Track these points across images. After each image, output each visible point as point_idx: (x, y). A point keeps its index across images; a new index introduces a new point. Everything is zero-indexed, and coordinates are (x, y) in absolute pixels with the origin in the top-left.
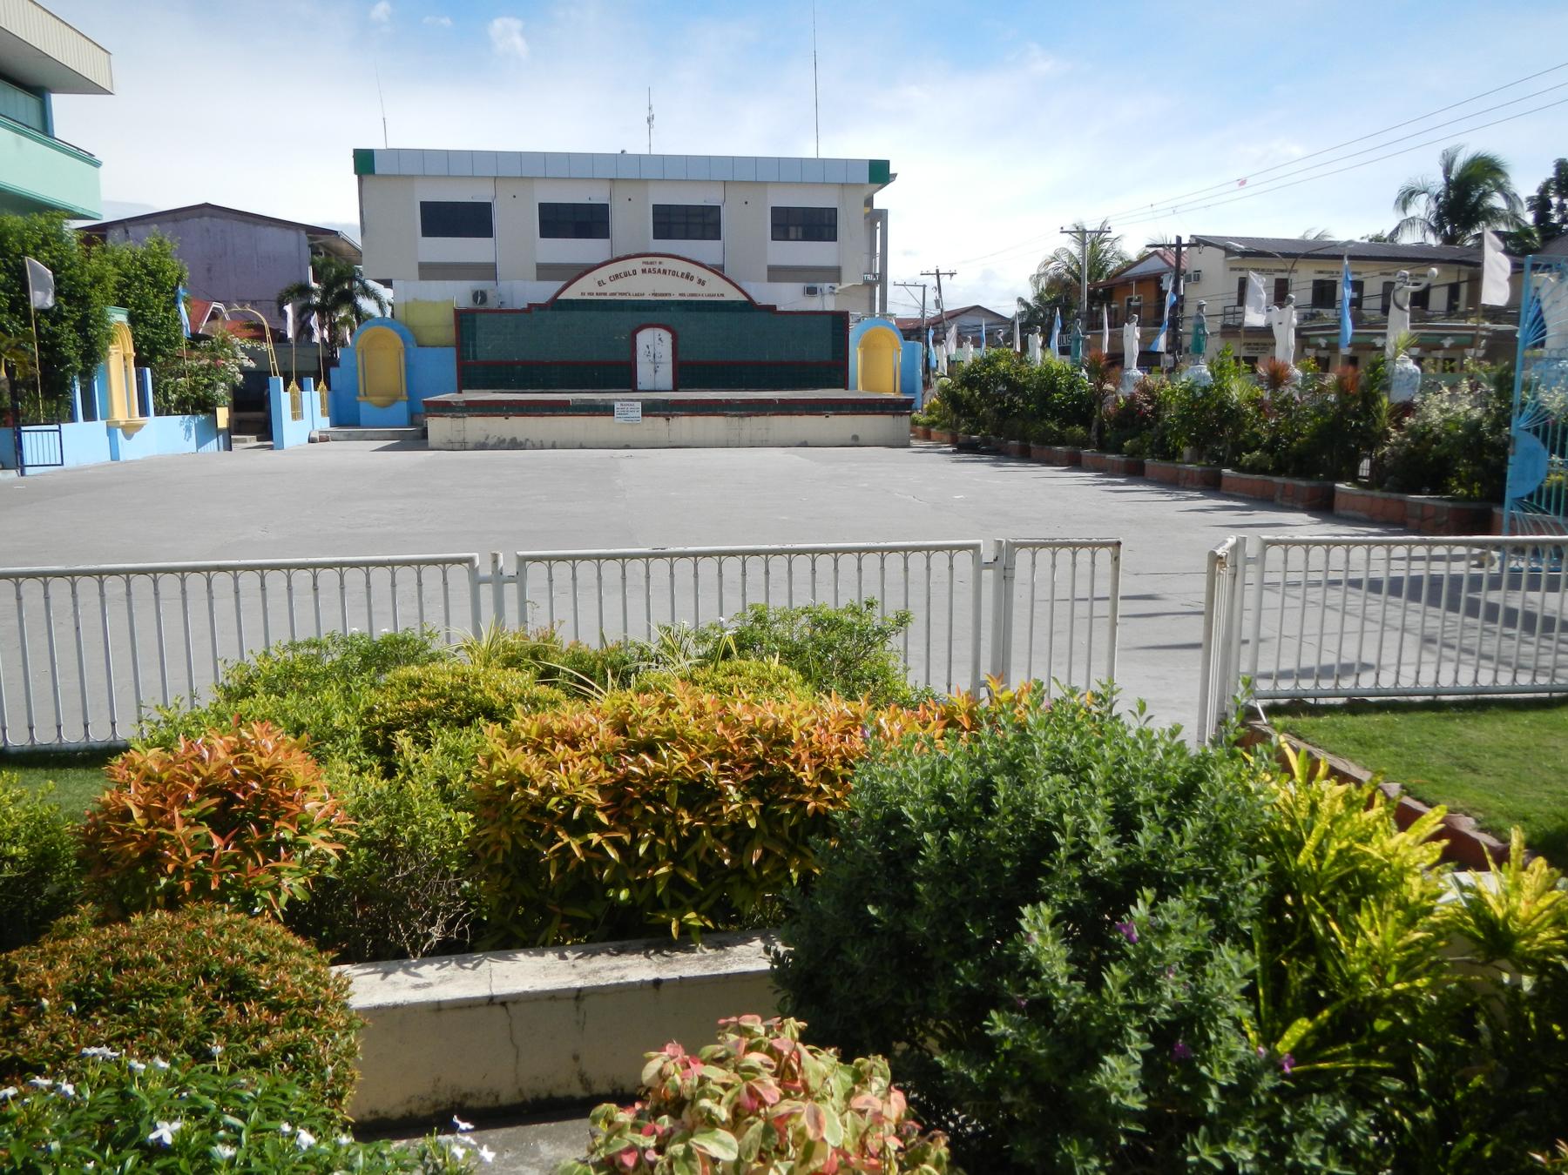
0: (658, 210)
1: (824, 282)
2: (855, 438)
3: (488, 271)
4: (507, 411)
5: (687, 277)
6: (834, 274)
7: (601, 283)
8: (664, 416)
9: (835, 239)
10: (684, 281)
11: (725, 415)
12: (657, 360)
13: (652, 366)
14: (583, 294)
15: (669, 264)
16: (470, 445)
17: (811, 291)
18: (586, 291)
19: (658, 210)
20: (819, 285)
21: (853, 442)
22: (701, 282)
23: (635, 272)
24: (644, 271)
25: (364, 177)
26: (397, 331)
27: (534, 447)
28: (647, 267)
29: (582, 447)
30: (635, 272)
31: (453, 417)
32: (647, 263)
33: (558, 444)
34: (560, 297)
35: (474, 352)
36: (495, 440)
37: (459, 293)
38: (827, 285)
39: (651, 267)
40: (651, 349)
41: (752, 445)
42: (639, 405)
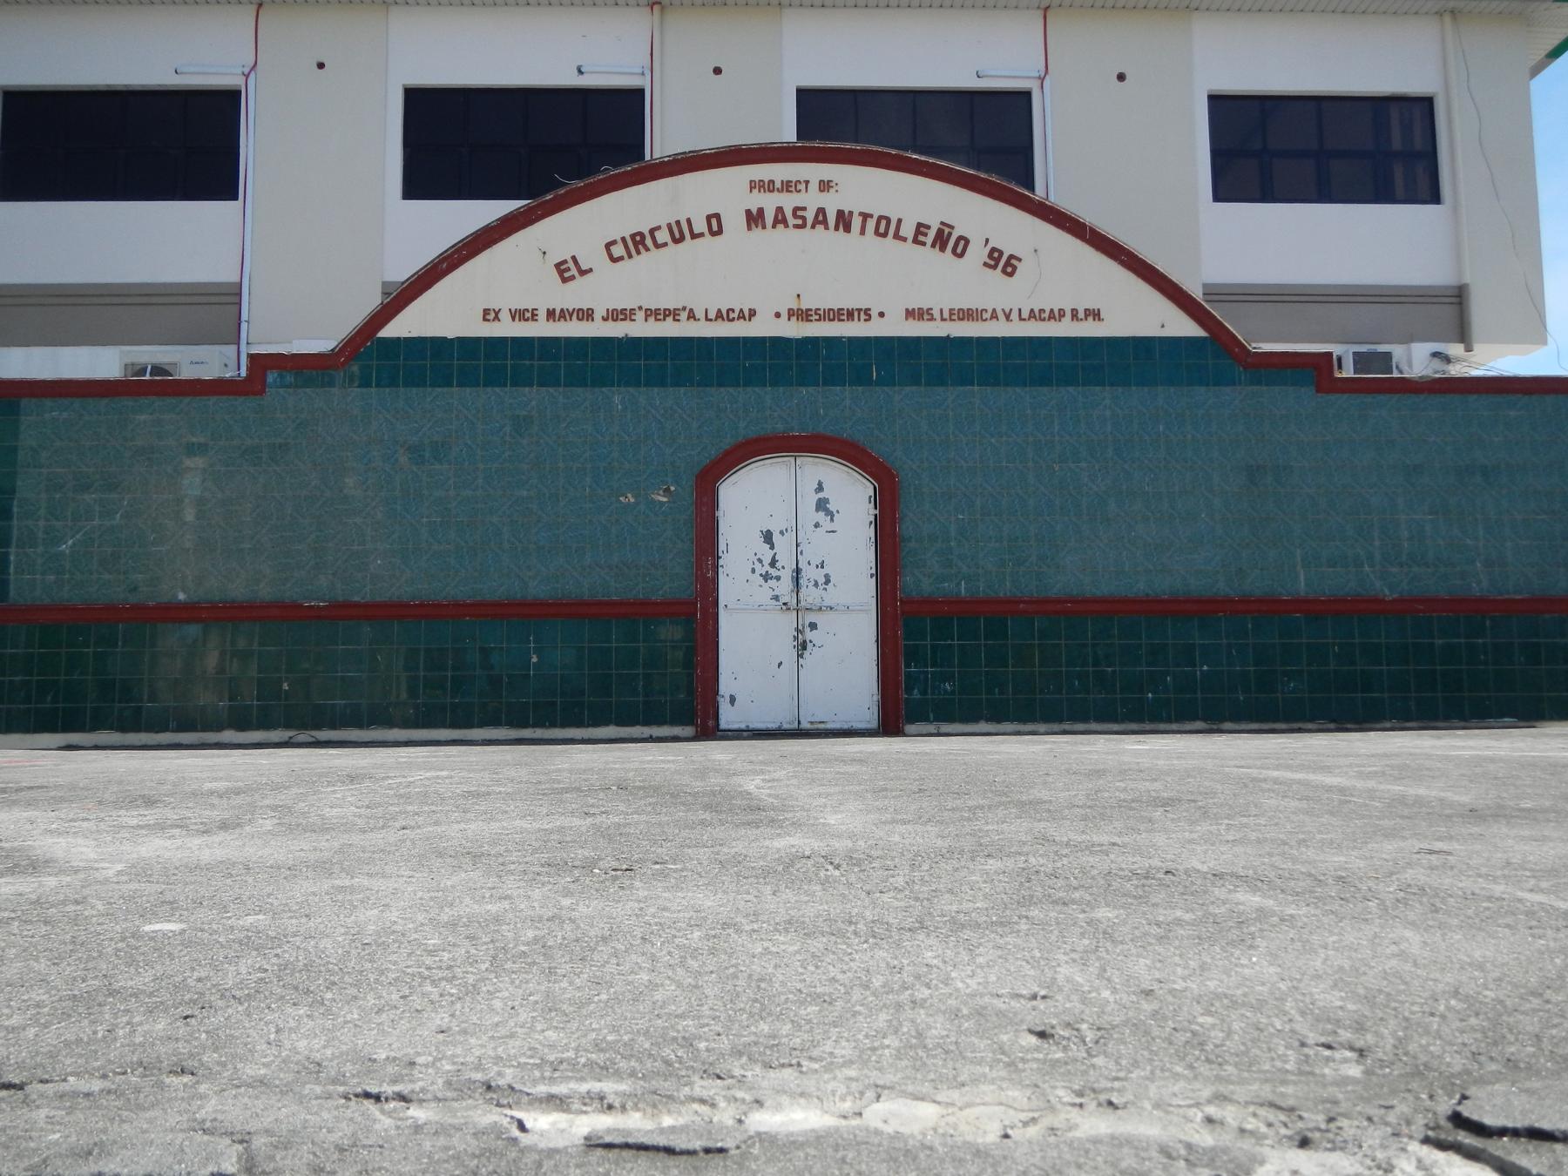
1: (1409, 339)
5: (941, 240)
9: (1433, 196)
10: (928, 254)
12: (810, 595)
13: (788, 622)
14: (489, 315)
18: (506, 303)
22: (1002, 262)
23: (715, 226)
24: (754, 219)
28: (769, 203)
32: (768, 187)
34: (390, 331)
39: (788, 201)
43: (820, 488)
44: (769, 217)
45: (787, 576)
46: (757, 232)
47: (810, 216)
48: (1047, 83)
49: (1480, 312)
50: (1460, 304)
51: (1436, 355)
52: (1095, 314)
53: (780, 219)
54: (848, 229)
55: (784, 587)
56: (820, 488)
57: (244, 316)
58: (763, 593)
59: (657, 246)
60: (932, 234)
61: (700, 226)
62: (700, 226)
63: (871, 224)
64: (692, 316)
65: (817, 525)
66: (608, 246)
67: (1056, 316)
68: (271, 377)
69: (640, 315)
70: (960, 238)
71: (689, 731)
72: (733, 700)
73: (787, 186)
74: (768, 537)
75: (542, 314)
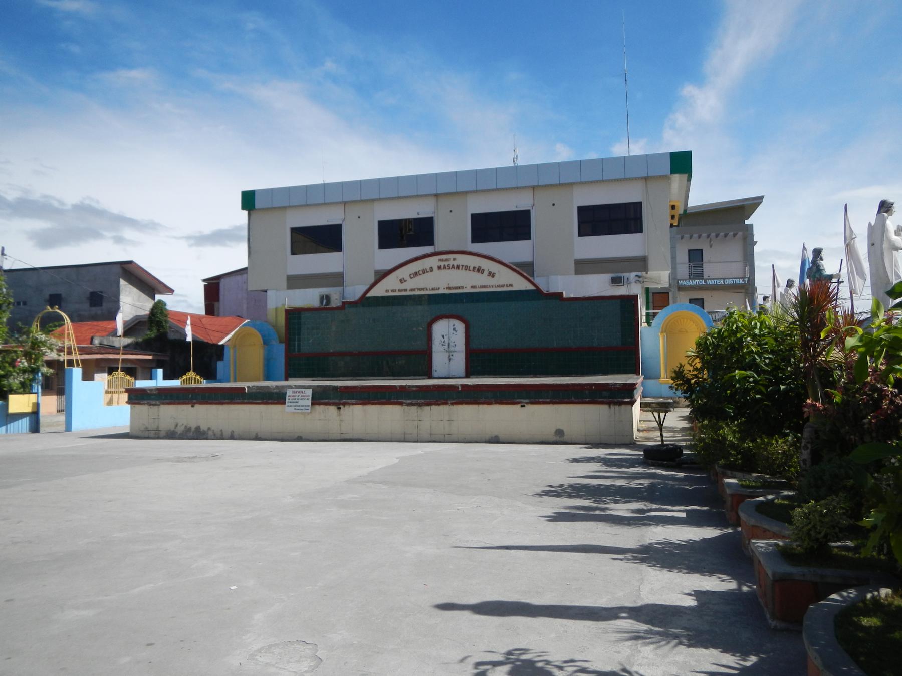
0: (476, 218)
1: (631, 272)
2: (559, 432)
3: (337, 279)
4: (192, 399)
5: (478, 271)
6: (641, 263)
7: (402, 281)
8: (333, 404)
9: (640, 230)
10: (476, 275)
11: (401, 404)
12: (452, 349)
14: (387, 291)
15: (462, 260)
16: (163, 434)
17: (616, 281)
18: (390, 288)
19: (476, 218)
20: (626, 275)
21: (557, 438)
22: (492, 275)
23: (432, 270)
25: (251, 212)
26: (258, 330)
27: (215, 438)
28: (442, 264)
29: (257, 438)
30: (432, 270)
31: (150, 404)
33: (236, 434)
34: (369, 295)
35: (299, 345)
36: (183, 428)
37: (308, 298)
38: (633, 275)
39: (446, 263)
40: (446, 339)
41: (433, 439)
42: (309, 392)
43: (454, 326)
44: (442, 267)
45: (447, 345)
46: (440, 270)
47: (451, 266)
48: (534, 208)
49: (651, 262)
50: (645, 261)
51: (636, 276)
52: (511, 285)
53: (445, 268)
54: (459, 269)
55: (446, 347)
56: (454, 326)
57: (345, 280)
58: (442, 348)
59: (420, 275)
60: (476, 269)
61: (428, 270)
62: (428, 270)
63: (464, 268)
64: (427, 290)
65: (453, 334)
66: (410, 275)
67: (503, 286)
68: (346, 306)
69: (416, 290)
70: (482, 270)
71: (427, 377)
72: (436, 371)
73: (447, 260)
74: (443, 336)
75: (397, 291)
